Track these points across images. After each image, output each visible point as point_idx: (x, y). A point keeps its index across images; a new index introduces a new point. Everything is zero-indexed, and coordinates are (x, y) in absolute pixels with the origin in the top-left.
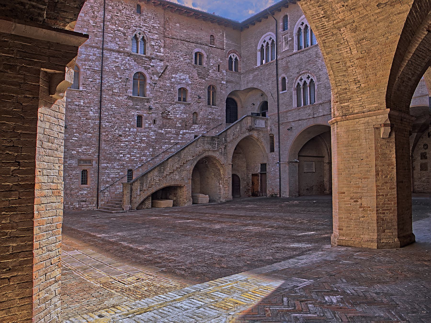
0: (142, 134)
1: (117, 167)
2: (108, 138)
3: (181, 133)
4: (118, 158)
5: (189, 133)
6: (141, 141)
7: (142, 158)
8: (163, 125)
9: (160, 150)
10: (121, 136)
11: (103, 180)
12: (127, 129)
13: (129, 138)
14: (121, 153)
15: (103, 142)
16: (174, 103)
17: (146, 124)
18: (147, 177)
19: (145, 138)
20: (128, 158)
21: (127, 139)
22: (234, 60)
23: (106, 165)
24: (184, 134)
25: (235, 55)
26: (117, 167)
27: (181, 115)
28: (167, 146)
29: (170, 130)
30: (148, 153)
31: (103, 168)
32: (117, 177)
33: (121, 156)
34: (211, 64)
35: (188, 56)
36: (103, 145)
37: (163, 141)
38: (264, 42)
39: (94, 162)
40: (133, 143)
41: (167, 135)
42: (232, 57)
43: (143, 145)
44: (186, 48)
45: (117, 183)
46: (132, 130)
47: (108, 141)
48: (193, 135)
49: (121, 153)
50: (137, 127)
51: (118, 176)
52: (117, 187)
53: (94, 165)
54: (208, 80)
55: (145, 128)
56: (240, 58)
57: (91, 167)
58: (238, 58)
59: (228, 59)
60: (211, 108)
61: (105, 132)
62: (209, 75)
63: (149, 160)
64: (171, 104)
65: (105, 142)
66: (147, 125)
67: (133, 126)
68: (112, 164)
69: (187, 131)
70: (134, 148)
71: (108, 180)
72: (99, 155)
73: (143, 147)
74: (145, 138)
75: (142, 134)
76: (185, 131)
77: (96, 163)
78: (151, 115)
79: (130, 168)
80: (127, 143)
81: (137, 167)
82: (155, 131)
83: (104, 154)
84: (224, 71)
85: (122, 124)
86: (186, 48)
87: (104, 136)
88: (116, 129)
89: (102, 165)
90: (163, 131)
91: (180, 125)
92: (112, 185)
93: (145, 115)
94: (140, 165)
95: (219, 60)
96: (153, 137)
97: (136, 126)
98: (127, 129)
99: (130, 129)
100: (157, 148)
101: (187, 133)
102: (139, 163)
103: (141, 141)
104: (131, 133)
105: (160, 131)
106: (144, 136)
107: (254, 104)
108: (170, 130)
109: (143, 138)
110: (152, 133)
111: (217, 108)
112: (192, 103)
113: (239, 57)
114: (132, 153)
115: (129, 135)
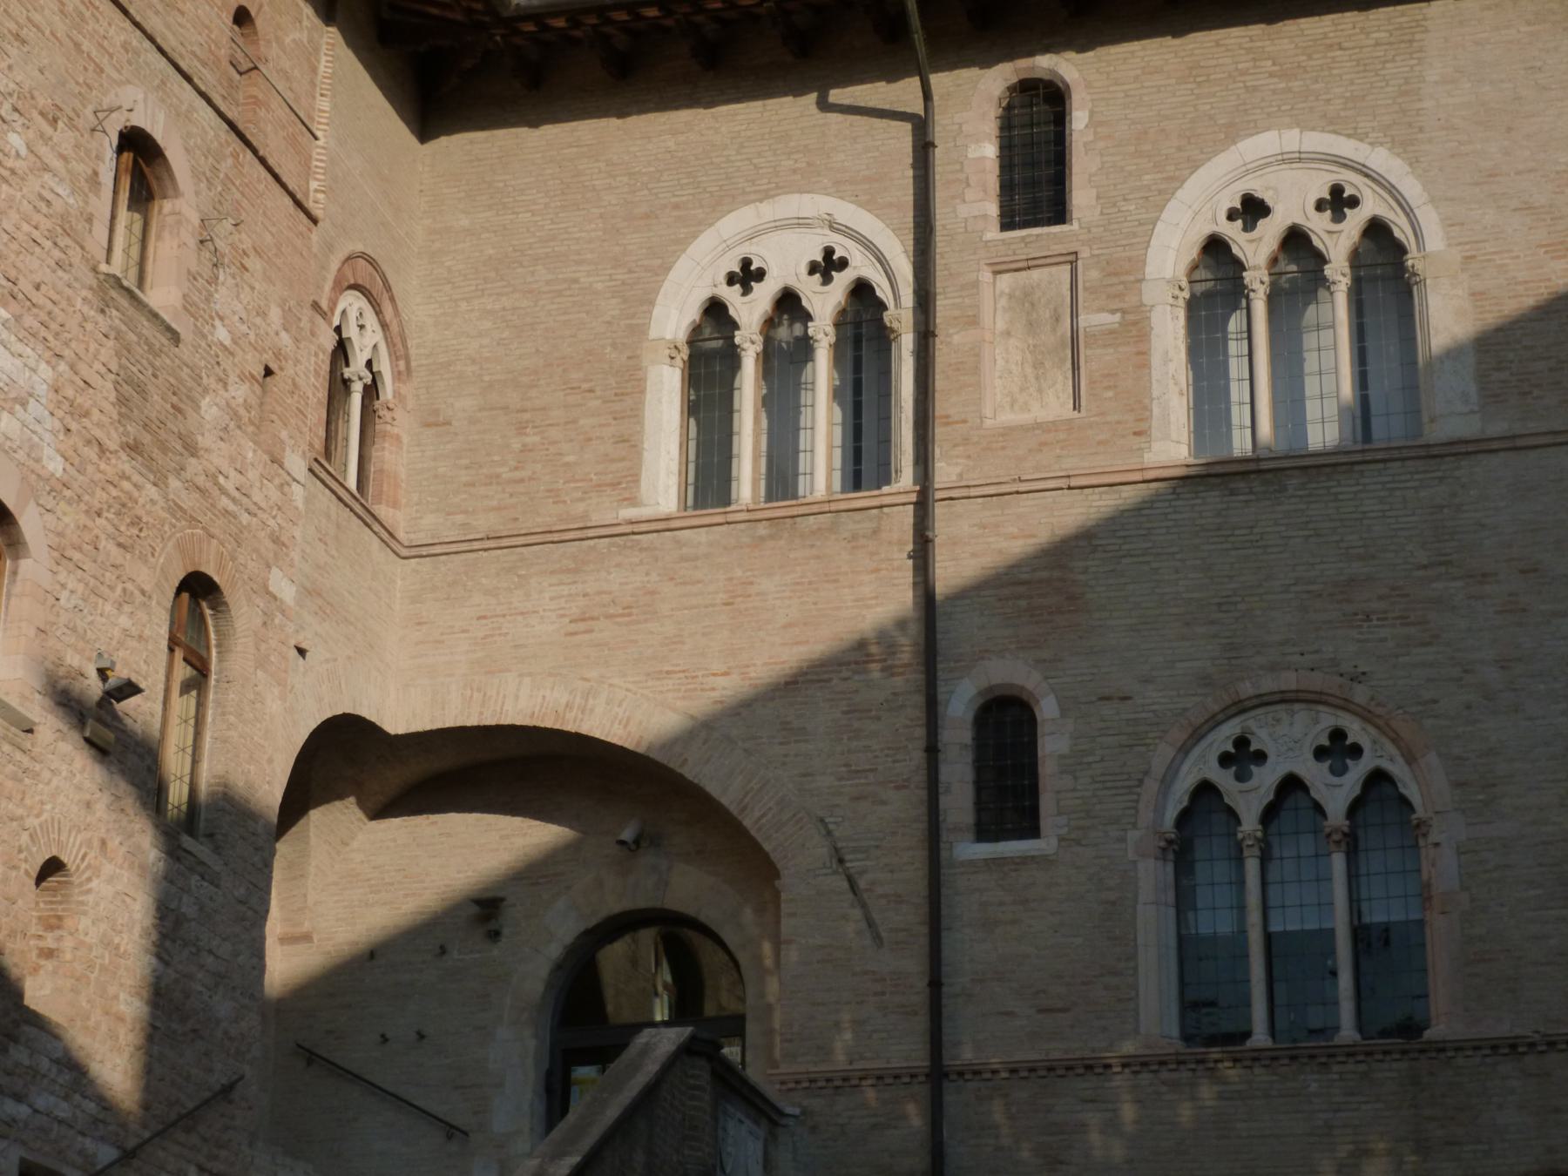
22: (356, 369)
25: (371, 320)
34: (222, 334)
35: (64, 137)
38: (747, 276)
42: (351, 332)
44: (61, 28)
54: (189, 501)
56: (397, 376)
58: (384, 366)
59: (329, 341)
62: (192, 449)
84: (297, 464)
86: (61, 28)
95: (275, 314)
113: (394, 357)
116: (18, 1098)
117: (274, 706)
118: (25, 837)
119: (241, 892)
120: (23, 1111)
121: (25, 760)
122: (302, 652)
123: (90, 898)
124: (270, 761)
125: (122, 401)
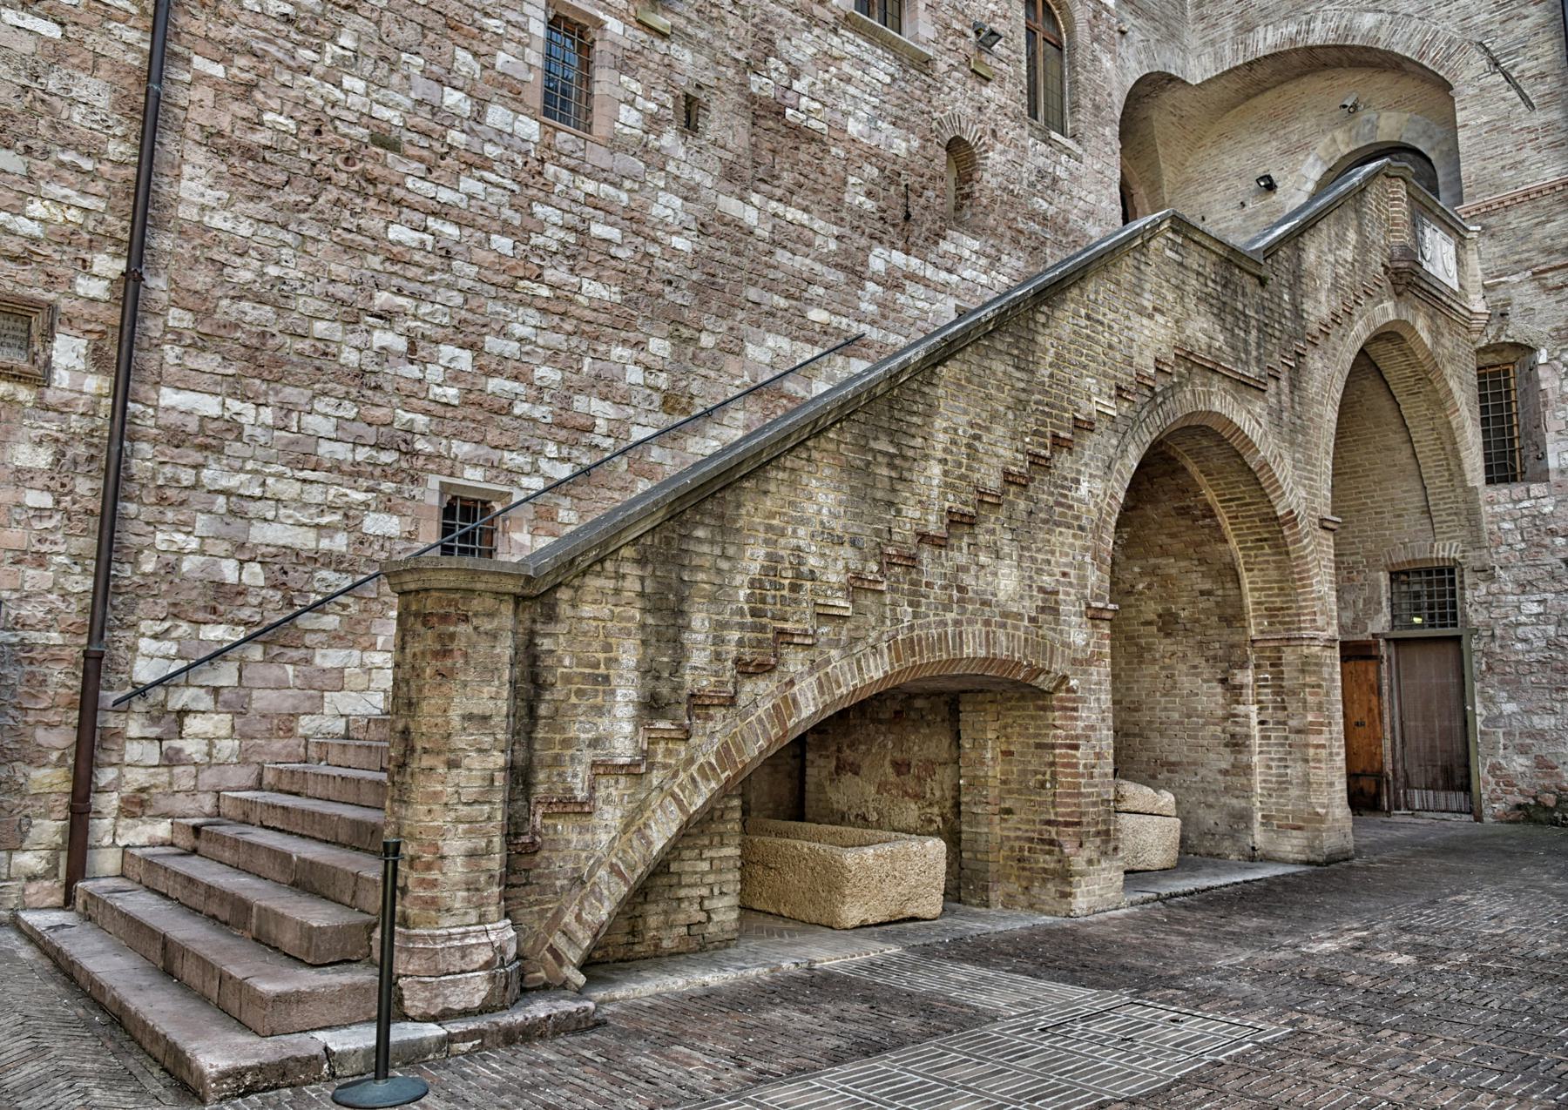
0: (590, 186)
1: (342, 452)
2: (256, 124)
3: (877, 264)
4: (350, 357)
5: (925, 282)
6: (581, 251)
7: (580, 403)
8: (756, 165)
9: (732, 364)
10: (385, 141)
11: (171, 569)
12: (452, 98)
13: (468, 184)
14: (386, 317)
15: (198, 155)
16: (830, 18)
17: (624, 104)
18: (726, 529)
19: (614, 234)
20: (455, 377)
21: (445, 195)
23: (209, 406)
24: (894, 282)
26: (342, 452)
28: (784, 344)
29: (803, 217)
30: (635, 375)
31: (176, 438)
32: (334, 561)
33: (381, 338)
36: (194, 187)
37: (753, 293)
39: (68, 352)
40: (503, 244)
41: (782, 256)
43: (593, 289)
45: (331, 621)
46: (497, 115)
47: (249, 153)
48: (952, 302)
49: (386, 316)
50: (547, 113)
51: (340, 543)
52: (329, 658)
53: (61, 378)
55: (615, 144)
57: (24, 394)
60: (1047, 141)
61: (226, 52)
63: (638, 434)
64: (812, 21)
65: (223, 153)
66: (628, 115)
67: (514, 94)
68: (286, 409)
69: (914, 262)
71: (228, 571)
72: (132, 281)
73: (599, 307)
74: (614, 234)
75: (590, 186)
76: (898, 258)
77: (97, 359)
78: (661, 46)
79: (473, 477)
80: (451, 230)
81: (537, 483)
82: (690, 193)
83: (201, 278)
85: (410, 34)
87: (203, 93)
89: (168, 397)
90: (750, 216)
91: (869, 205)
92: (263, 635)
93: (614, 26)
94: (564, 471)
96: (679, 243)
97: (535, 98)
98: (452, 98)
99: (481, 104)
100: (707, 340)
101: (913, 277)
102: (551, 449)
103: (581, 251)
104: (491, 150)
105: (731, 206)
106: (605, 209)
107: (1270, 186)
108: (803, 217)
109: (597, 230)
110: (667, 206)
111: (1078, 159)
112: (942, 67)
114: (492, 343)
115: (476, 164)
116: (950, 271)
117: (1107, 62)
118: (935, 124)
119: (1097, 167)
120: (955, 278)
121: (929, 80)
122: (1123, 33)
123: (989, 162)
124: (1110, 95)
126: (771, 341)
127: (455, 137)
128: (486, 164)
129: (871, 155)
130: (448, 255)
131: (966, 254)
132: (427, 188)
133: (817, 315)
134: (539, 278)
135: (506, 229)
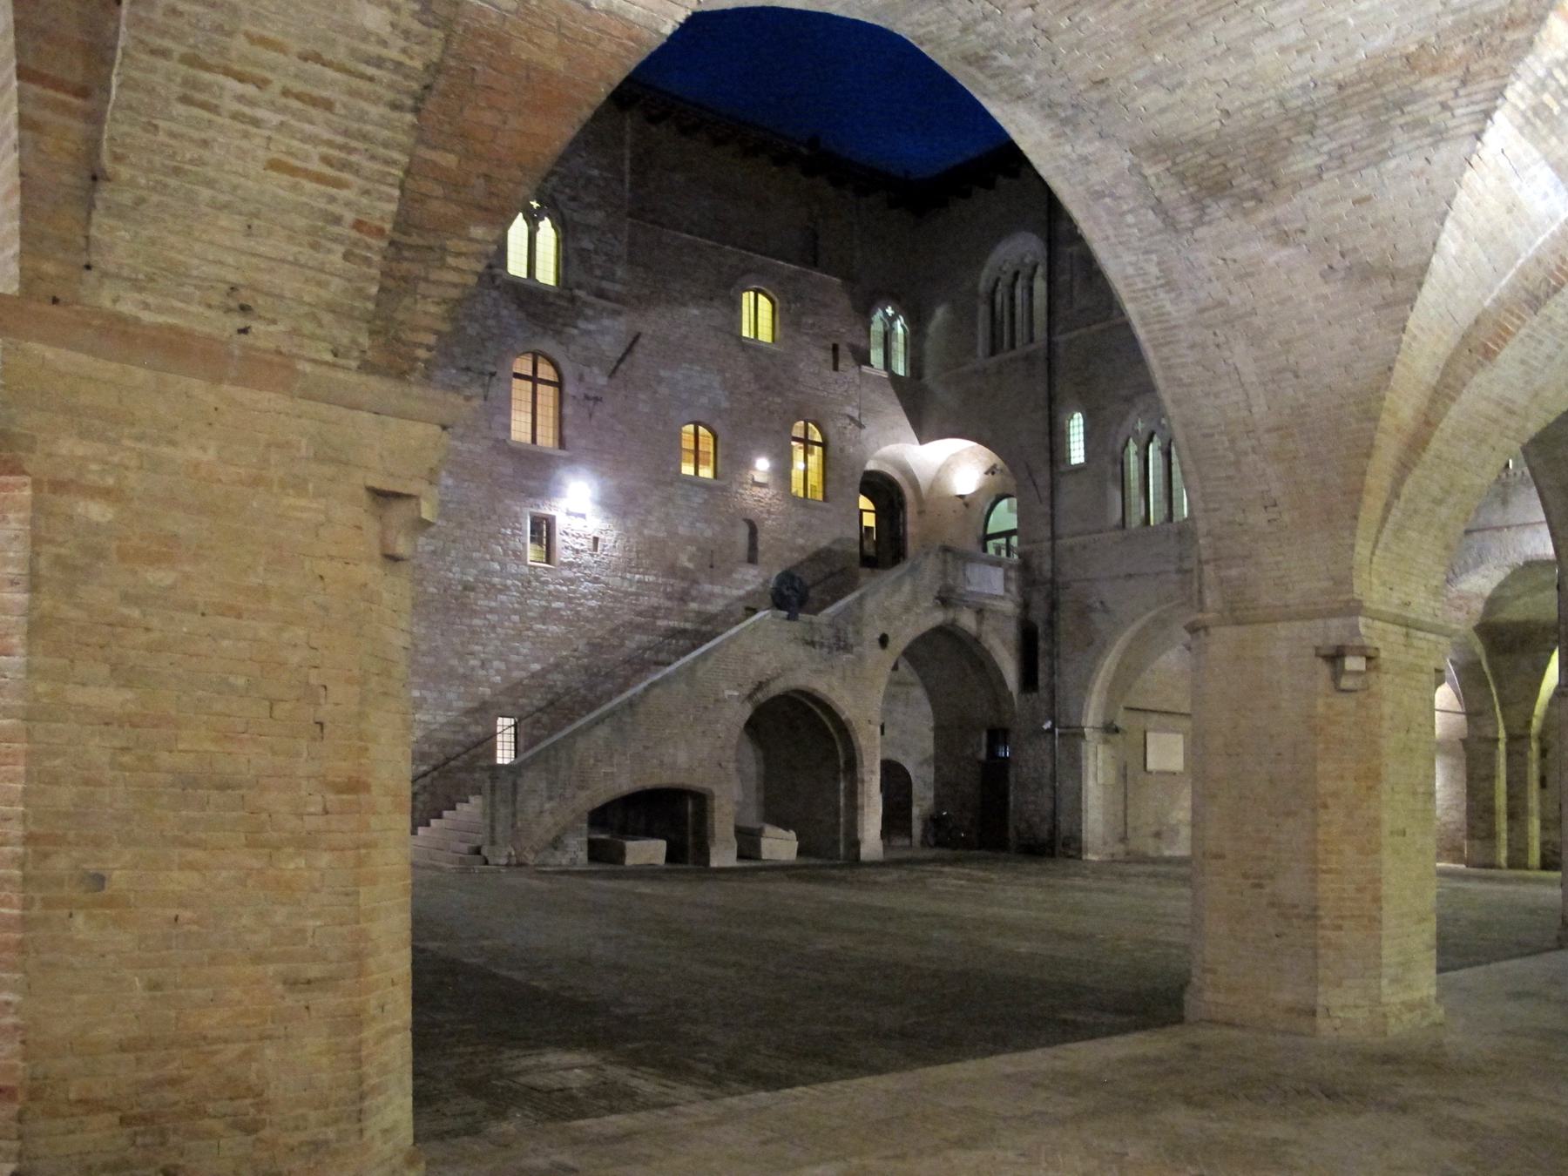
6: (547, 615)
10: (468, 587)
13: (502, 597)
21: (493, 604)
27: (692, 524)
40: (516, 618)
70: (519, 637)
85: (477, 544)
88: (453, 563)
103: (547, 615)
125: (758, 378)
126: (637, 637)
127: (496, 580)
128: (507, 588)
129: (691, 540)
130: (494, 627)
131: (748, 577)
132: (486, 603)
133: (661, 623)
134: (530, 629)
135: (515, 612)
